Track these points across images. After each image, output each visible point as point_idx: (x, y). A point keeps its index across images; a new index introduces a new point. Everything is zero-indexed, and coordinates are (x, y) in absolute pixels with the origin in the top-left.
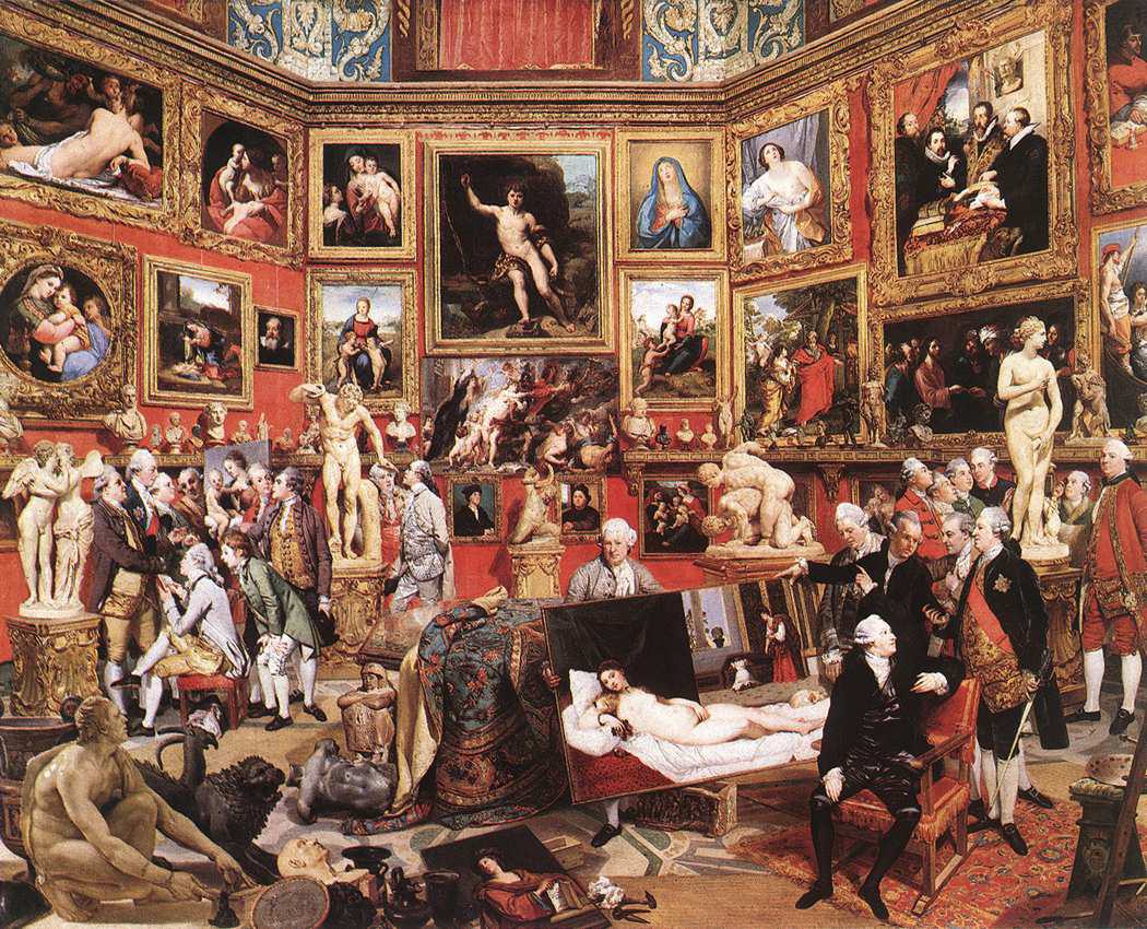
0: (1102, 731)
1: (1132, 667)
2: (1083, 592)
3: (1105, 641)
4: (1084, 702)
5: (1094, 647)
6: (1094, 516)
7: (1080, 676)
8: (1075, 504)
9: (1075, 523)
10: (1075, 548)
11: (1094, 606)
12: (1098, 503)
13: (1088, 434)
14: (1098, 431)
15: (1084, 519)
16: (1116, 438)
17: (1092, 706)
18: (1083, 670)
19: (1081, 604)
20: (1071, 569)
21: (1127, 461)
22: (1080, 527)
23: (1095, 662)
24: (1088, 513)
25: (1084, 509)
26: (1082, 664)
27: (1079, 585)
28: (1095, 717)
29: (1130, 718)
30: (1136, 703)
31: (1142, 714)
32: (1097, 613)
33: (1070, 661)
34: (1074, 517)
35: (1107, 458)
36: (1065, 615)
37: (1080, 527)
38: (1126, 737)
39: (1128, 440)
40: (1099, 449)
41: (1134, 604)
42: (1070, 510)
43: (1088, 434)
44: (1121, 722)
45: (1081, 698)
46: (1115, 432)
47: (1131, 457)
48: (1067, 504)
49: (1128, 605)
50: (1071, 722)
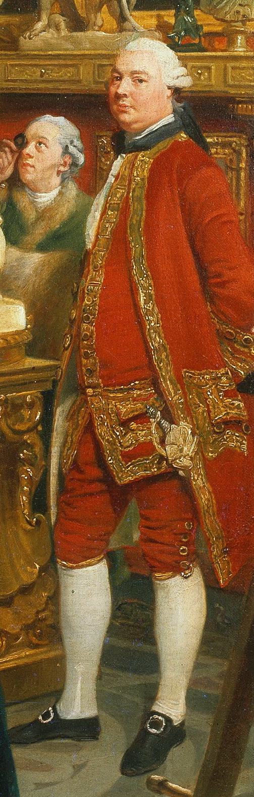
0: (104, 760)
1: (181, 608)
2: (59, 421)
3: (114, 543)
4: (57, 694)
5: (81, 557)
6: (91, 231)
7: (49, 629)
8: (45, 198)
9: (41, 248)
10: (42, 313)
11: (89, 454)
12: (100, 200)
13: (78, 24)
14: (104, 17)
15: (64, 236)
16: (148, 33)
17: (78, 702)
18: (57, 613)
19: (55, 450)
20: (31, 362)
21: (177, 92)
22: (56, 257)
23: (88, 593)
24: (76, 222)
25: (65, 211)
26: (55, 599)
27: (48, 401)
28: (87, 729)
29: (175, 734)
30: (193, 699)
31: (204, 723)
32: (96, 473)
33: (26, 590)
34: (39, 233)
35: (125, 86)
36: (13, 477)
37: (56, 257)
38: (162, 785)
39: (181, 41)
40: (107, 64)
41: (190, 449)
42: (31, 215)
43: (78, 24)
44: (147, 749)
45: (49, 680)
46: (149, 18)
47: (185, 82)
48: (23, 200)
49: (169, 451)
50: (24, 742)
